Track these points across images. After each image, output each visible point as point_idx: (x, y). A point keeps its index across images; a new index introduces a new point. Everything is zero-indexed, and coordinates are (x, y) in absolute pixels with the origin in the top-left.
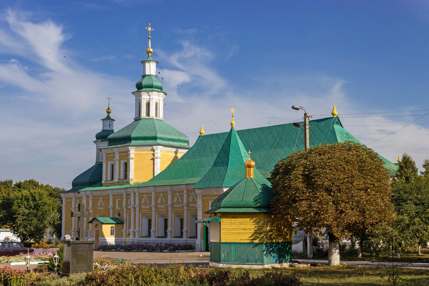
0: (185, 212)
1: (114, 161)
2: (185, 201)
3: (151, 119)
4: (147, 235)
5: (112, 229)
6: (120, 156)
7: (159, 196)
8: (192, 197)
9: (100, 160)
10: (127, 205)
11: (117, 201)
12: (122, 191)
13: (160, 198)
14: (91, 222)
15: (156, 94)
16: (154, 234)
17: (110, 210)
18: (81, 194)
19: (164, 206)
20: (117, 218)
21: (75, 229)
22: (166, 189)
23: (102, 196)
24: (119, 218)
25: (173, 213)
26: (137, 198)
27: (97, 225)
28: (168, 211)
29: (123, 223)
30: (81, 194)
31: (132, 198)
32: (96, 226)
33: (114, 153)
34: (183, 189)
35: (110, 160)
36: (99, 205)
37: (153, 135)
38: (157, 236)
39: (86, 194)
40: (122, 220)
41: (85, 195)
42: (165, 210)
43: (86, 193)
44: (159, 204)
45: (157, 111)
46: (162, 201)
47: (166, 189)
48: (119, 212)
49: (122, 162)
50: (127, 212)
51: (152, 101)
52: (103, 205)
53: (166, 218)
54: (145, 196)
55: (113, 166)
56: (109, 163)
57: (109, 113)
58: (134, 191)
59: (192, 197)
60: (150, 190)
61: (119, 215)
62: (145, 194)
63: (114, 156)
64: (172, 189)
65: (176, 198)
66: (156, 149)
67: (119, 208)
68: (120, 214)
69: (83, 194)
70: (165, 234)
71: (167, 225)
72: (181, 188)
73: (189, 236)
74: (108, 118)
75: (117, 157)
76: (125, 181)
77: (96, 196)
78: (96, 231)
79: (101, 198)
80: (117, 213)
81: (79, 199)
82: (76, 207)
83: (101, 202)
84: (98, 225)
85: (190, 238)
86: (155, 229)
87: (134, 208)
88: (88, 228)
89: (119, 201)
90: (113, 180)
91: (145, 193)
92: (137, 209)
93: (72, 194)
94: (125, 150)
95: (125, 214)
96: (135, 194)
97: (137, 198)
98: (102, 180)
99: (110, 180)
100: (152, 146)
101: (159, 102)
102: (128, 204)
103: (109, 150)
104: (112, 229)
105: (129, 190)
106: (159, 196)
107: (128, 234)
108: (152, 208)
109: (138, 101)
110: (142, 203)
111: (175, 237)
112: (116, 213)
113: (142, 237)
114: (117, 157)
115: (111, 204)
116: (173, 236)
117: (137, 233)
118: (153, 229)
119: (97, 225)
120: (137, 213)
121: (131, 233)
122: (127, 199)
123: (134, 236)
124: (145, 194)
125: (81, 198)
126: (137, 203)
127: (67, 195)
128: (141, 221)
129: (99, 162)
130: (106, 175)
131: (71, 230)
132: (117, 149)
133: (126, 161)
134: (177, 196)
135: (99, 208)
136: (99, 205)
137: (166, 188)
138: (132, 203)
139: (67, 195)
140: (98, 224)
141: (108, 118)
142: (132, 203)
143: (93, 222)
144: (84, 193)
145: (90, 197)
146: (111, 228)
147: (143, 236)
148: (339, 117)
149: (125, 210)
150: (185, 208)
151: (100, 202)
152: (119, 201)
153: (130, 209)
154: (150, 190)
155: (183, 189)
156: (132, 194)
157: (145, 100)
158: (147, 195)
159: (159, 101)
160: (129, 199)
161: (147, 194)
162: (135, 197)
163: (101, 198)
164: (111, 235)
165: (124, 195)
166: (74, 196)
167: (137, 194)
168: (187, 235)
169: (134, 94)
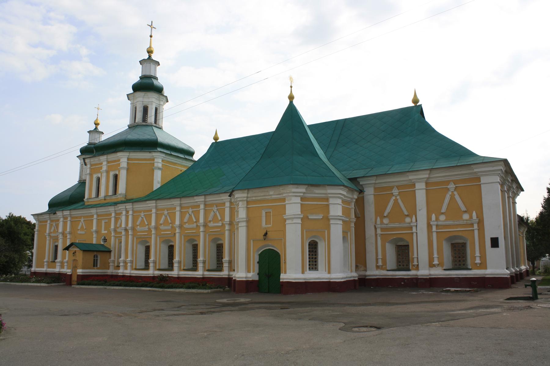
0: (202, 235)
1: (102, 173)
2: (201, 220)
4: (143, 267)
5: (96, 258)
6: (108, 167)
7: (163, 214)
8: (212, 213)
9: (84, 178)
11: (103, 222)
12: (110, 210)
14: (67, 248)
15: (156, 97)
16: (154, 265)
17: (93, 234)
18: (58, 214)
19: (169, 227)
20: (103, 244)
21: (49, 259)
22: (173, 204)
23: (84, 217)
24: (104, 244)
25: (183, 237)
26: (130, 217)
27: (75, 252)
28: (175, 234)
29: (110, 252)
30: (58, 214)
31: (123, 218)
32: (74, 253)
33: (102, 163)
36: (79, 228)
38: (157, 268)
39: (63, 215)
40: (110, 248)
42: (170, 232)
44: (162, 225)
46: (166, 219)
48: (105, 237)
49: (112, 174)
51: (152, 104)
53: (171, 244)
54: (142, 214)
55: (99, 180)
57: (97, 124)
59: (212, 213)
60: (149, 207)
61: (105, 240)
62: (142, 212)
63: (102, 167)
65: (187, 216)
67: (106, 232)
68: (106, 240)
69: (59, 215)
70: (169, 266)
71: (173, 253)
73: (207, 268)
74: (96, 130)
75: (104, 168)
76: (114, 197)
77: (76, 217)
78: (74, 260)
79: (82, 220)
80: (103, 238)
81: (55, 222)
82: (51, 231)
83: (82, 225)
84: (77, 253)
85: (208, 270)
86: (156, 258)
87: (126, 230)
88: (64, 257)
89: (105, 222)
90: (99, 197)
91: (142, 211)
92: (130, 233)
93: (47, 216)
95: (113, 238)
96: (127, 212)
97: (130, 217)
98: (84, 198)
99: (95, 197)
100: (151, 153)
102: (118, 225)
103: (96, 160)
104: (96, 258)
105: (120, 208)
106: (163, 214)
107: (116, 265)
108: (152, 231)
110: (138, 223)
111: (184, 270)
112: (102, 238)
113: (136, 269)
114: (104, 168)
115: (94, 228)
116: (182, 268)
117: (129, 264)
118: (152, 259)
119: (75, 252)
120: (130, 237)
121: (121, 264)
122: (116, 220)
123: (126, 268)
124: (142, 212)
125: (58, 220)
126: (130, 225)
127: (41, 218)
128: (135, 249)
129: (83, 179)
130: (89, 193)
131: (45, 260)
132: (103, 160)
133: (117, 173)
134: (189, 213)
135: (79, 232)
136: (79, 228)
138: (123, 226)
139: (41, 218)
140: (76, 251)
141: (96, 130)
142: (123, 226)
143: (70, 249)
144: (62, 214)
146: (94, 257)
147: (137, 268)
148: (422, 106)
150: (202, 229)
151: (81, 224)
152: (105, 222)
153: (121, 233)
154: (149, 205)
155: (198, 203)
156: (124, 213)
158: (144, 213)
159: (158, 105)
160: (120, 221)
161: (144, 211)
162: (127, 217)
163: (82, 220)
164: (94, 266)
165: (113, 215)
166: (50, 218)
167: (131, 213)
168: (204, 267)
169: (129, 96)
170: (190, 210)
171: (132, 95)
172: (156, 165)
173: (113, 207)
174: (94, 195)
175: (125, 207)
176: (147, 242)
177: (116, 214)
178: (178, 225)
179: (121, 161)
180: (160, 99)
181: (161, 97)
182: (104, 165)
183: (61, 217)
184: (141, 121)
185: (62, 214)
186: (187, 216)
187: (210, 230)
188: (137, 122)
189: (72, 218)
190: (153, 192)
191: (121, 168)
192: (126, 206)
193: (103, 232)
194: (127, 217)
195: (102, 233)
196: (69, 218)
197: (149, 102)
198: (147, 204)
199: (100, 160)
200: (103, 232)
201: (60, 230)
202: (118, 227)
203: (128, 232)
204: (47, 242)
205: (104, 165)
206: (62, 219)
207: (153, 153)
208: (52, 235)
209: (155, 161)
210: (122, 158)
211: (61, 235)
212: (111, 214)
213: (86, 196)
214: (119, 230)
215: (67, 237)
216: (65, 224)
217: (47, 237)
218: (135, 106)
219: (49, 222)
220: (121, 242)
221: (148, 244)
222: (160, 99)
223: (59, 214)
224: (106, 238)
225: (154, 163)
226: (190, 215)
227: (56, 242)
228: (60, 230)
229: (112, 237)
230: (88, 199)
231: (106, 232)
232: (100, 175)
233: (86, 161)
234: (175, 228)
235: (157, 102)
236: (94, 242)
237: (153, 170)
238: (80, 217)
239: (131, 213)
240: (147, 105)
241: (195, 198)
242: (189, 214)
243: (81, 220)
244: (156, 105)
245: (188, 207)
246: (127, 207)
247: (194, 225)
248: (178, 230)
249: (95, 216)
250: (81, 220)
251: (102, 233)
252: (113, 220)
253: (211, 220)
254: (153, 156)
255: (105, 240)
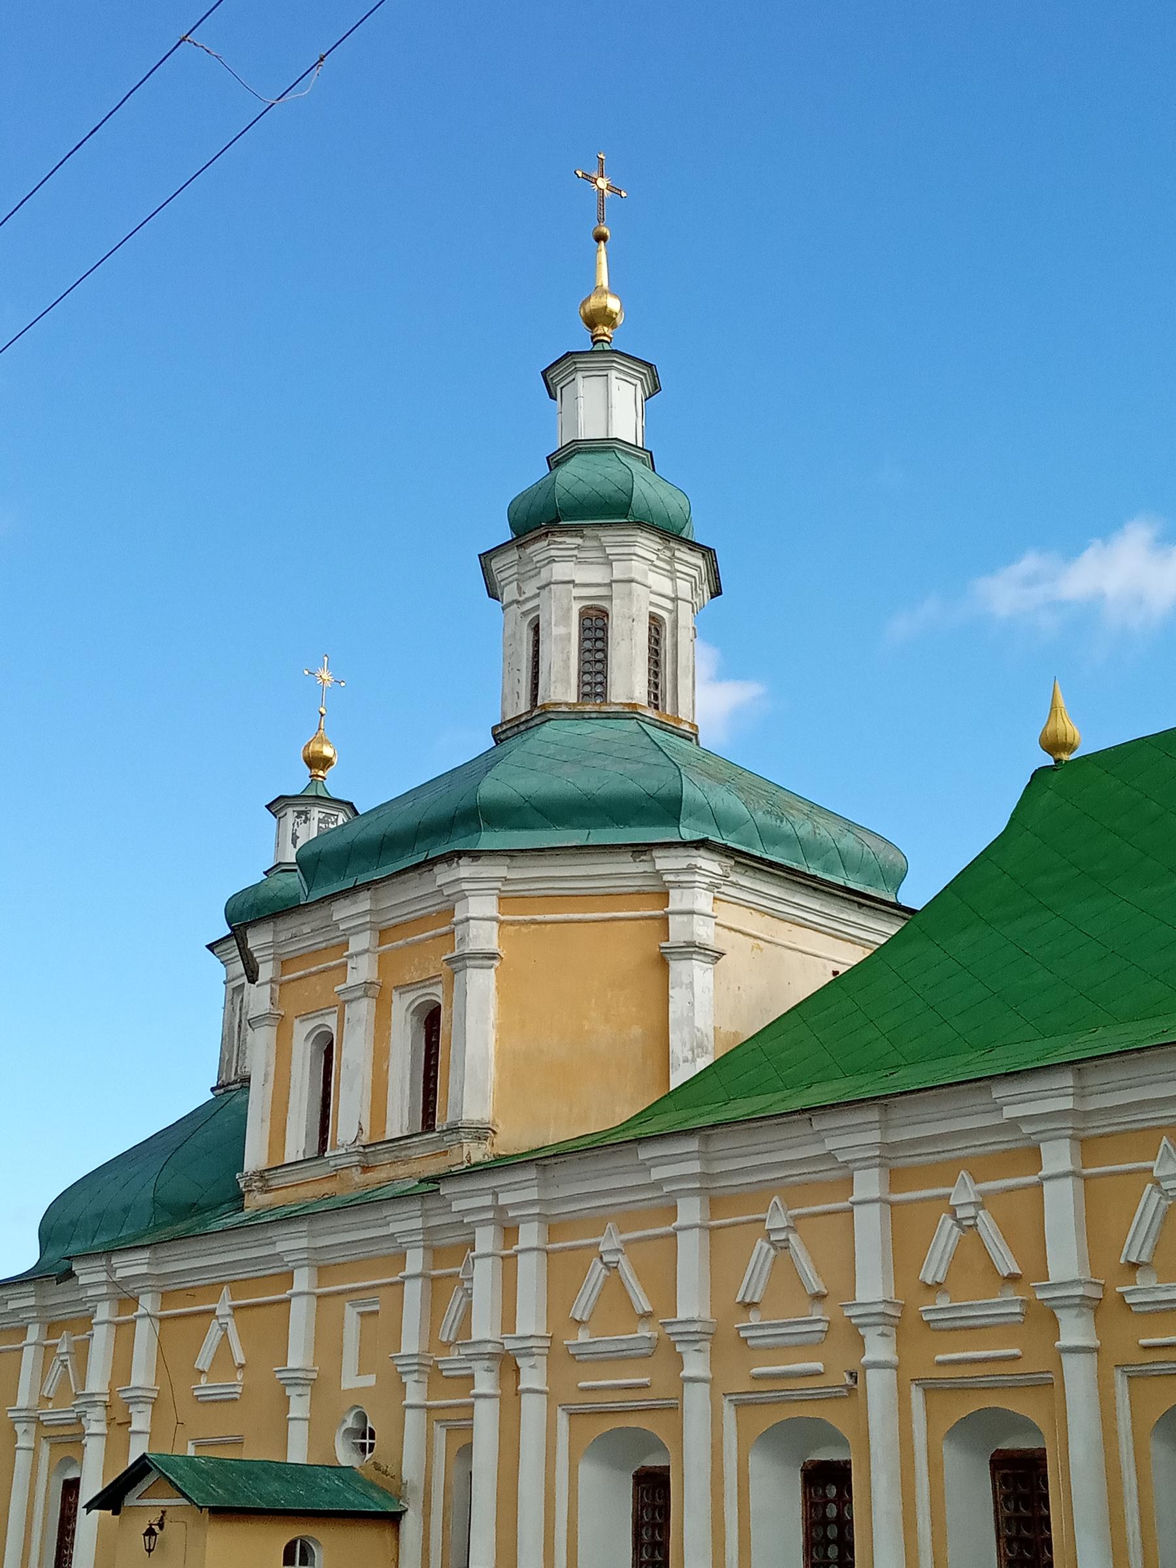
3: (617, 716)
10: (435, 1343)
12: (393, 1228)
13: (761, 1244)
22: (829, 1156)
26: (530, 1269)
29: (394, 1519)
33: (345, 945)
34: (1026, 1129)
35: (304, 1017)
37: (655, 782)
41: (104, 1290)
43: (111, 1271)
45: (656, 674)
47: (830, 1144)
48: (362, 1418)
50: (429, 1409)
52: (240, 1358)
55: (327, 1051)
56: (301, 1030)
58: (502, 1209)
60: (657, 1184)
61: (363, 1437)
64: (893, 1146)
65: (946, 1236)
66: (679, 885)
67: (370, 1380)
68: (372, 1436)
72: (1010, 1112)
75: (362, 970)
79: (223, 1307)
80: (350, 1422)
89: (361, 1314)
92: (532, 1377)
94: (430, 906)
95: (413, 1422)
97: (530, 1269)
101: (674, 612)
103: (306, 929)
109: (525, 614)
114: (362, 970)
115: (298, 1357)
125: (86, 1322)
133: (437, 993)
137: (830, 1144)
142: (484, 1328)
145: (142, 1299)
149: (415, 1393)
152: (362, 1315)
154: (657, 1174)
155: (1026, 1129)
156: (486, 1240)
157: (577, 592)
159: (669, 604)
163: (223, 1307)
170: (963, 1192)
171: (513, 555)
172: (678, 931)
173: (415, 1207)
174: (297, 1144)
175: (487, 1201)
176: (656, 1445)
177: (435, 1253)
178: (880, 1308)
179: (458, 916)
180: (678, 566)
181: (677, 554)
182: (357, 954)
183: (99, 1298)
184: (573, 699)
185: (103, 1277)
186: (946, 1236)
187: (1143, 1342)
188: (543, 706)
189: (167, 1297)
190: (670, 1095)
191: (463, 957)
192: (495, 1195)
193: (351, 1380)
194: (509, 1263)
195: (345, 1386)
196: (147, 1304)
197: (610, 585)
198: (645, 1166)
199: (336, 924)
200: (351, 1380)
201: (97, 1382)
202: (448, 1345)
203: (518, 1370)
204: (22, 1460)
205: (357, 954)
206: (104, 1312)
207: (656, 853)
208: (51, 1413)
209: (671, 908)
210: (463, 896)
211: (98, 1412)
212: (400, 1259)
213: (255, 1157)
214: (452, 1362)
215: (130, 1423)
216: (124, 1330)
217: (19, 1428)
218: (534, 615)
219: (34, 1333)
220: (466, 1452)
221: (653, 1461)
222: (678, 566)
223: (88, 1274)
224: (369, 1425)
225: (665, 919)
226: (969, 1228)
227: (70, 1462)
228: (97, 1382)
229: (409, 1413)
230: (261, 1175)
231: (370, 1380)
232: (331, 1022)
233: (251, 944)
234: (858, 1326)
235: (662, 584)
236: (297, 1453)
237: (662, 962)
238: (213, 1291)
239: (530, 1235)
240: (603, 604)
241: (999, 1092)
242: (958, 1222)
243: (213, 1311)
244: (651, 603)
245: (945, 1173)
246: (504, 1199)
247: (1008, 1303)
248: (879, 1348)
249: (302, 1280)
250: (213, 1311)
251: (345, 1386)
252: (413, 1292)
253: (1144, 1258)
254: (658, 874)
255: (363, 1437)
